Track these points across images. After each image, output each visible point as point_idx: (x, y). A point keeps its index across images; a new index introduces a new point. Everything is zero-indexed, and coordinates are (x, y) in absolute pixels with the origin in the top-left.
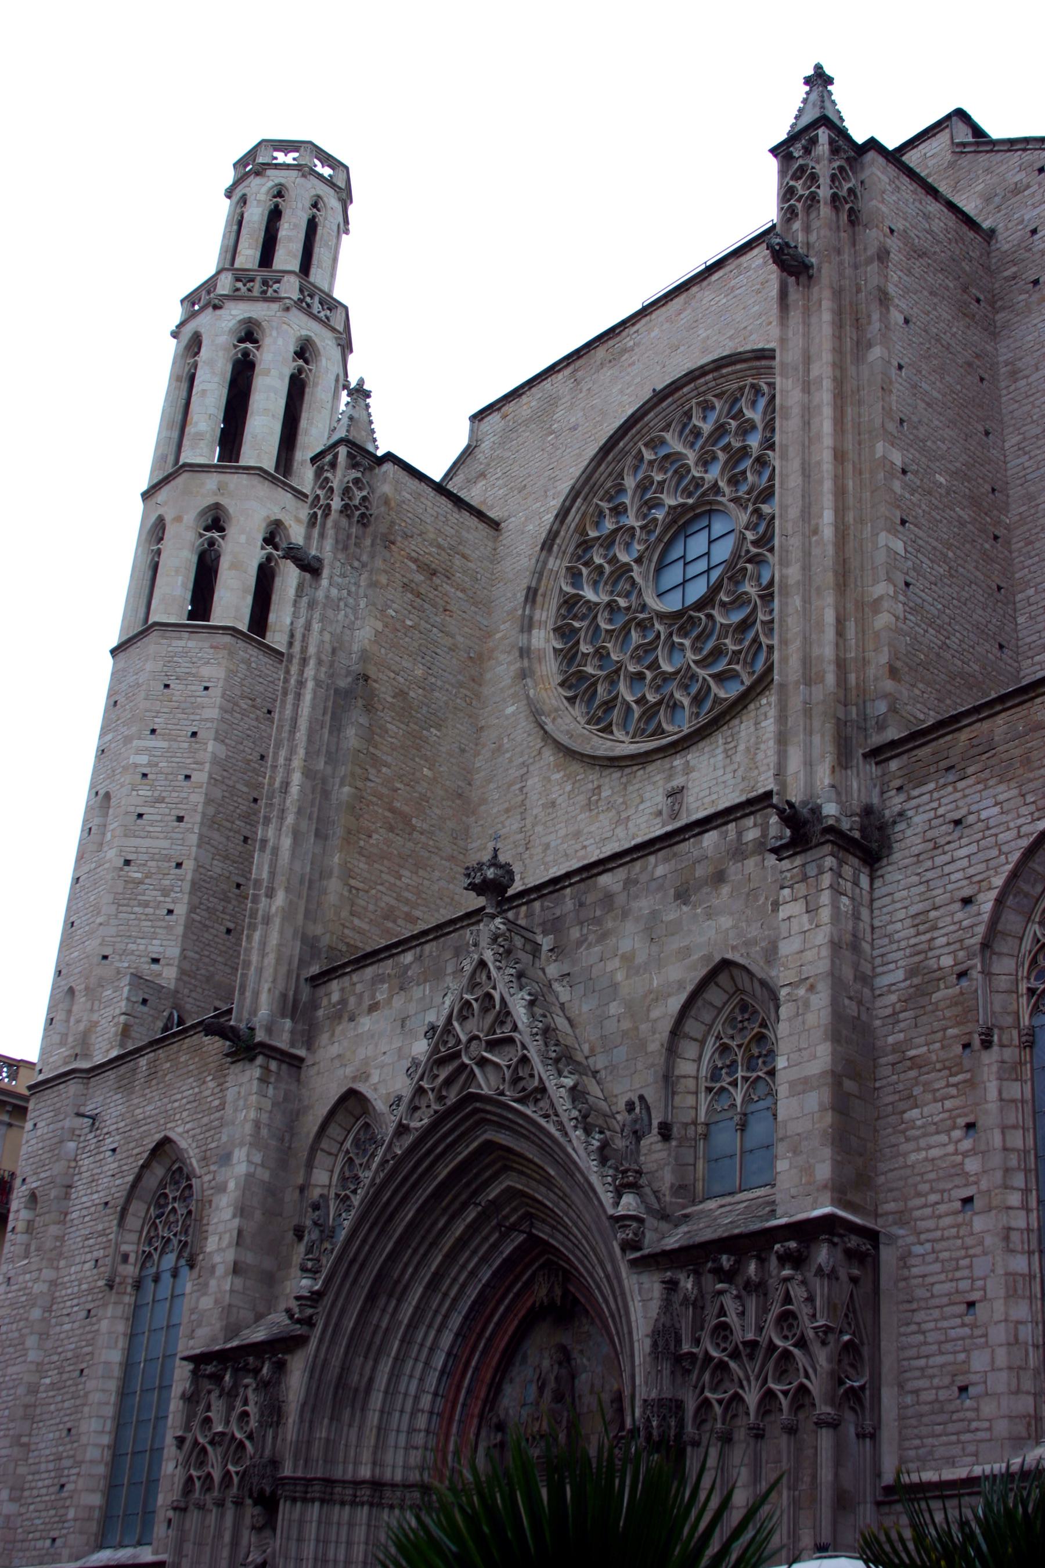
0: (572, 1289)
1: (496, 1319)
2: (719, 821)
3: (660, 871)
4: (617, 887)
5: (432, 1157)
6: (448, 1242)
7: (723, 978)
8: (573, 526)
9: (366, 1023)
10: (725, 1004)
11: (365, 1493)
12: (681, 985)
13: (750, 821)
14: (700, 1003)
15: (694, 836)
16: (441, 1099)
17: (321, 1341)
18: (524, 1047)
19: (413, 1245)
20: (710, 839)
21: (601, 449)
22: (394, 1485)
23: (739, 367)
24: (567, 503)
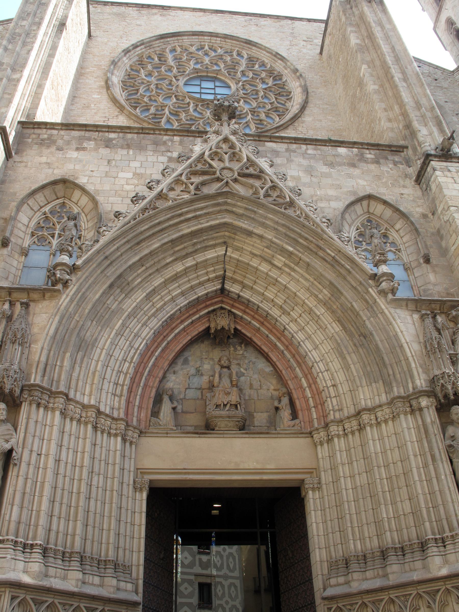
0: (239, 327)
1: (177, 331)
2: (347, 145)
3: (310, 152)
4: (279, 149)
5: (182, 218)
6: (169, 273)
7: (365, 203)
8: (137, 53)
9: (74, 154)
10: (361, 215)
11: (92, 414)
12: (337, 199)
13: (367, 152)
14: (352, 208)
15: (332, 146)
16: (197, 189)
17: (72, 301)
18: (272, 182)
19: (148, 265)
20: (342, 150)
21: (160, 35)
22: (107, 415)
23: (234, 42)
24: (138, 44)
